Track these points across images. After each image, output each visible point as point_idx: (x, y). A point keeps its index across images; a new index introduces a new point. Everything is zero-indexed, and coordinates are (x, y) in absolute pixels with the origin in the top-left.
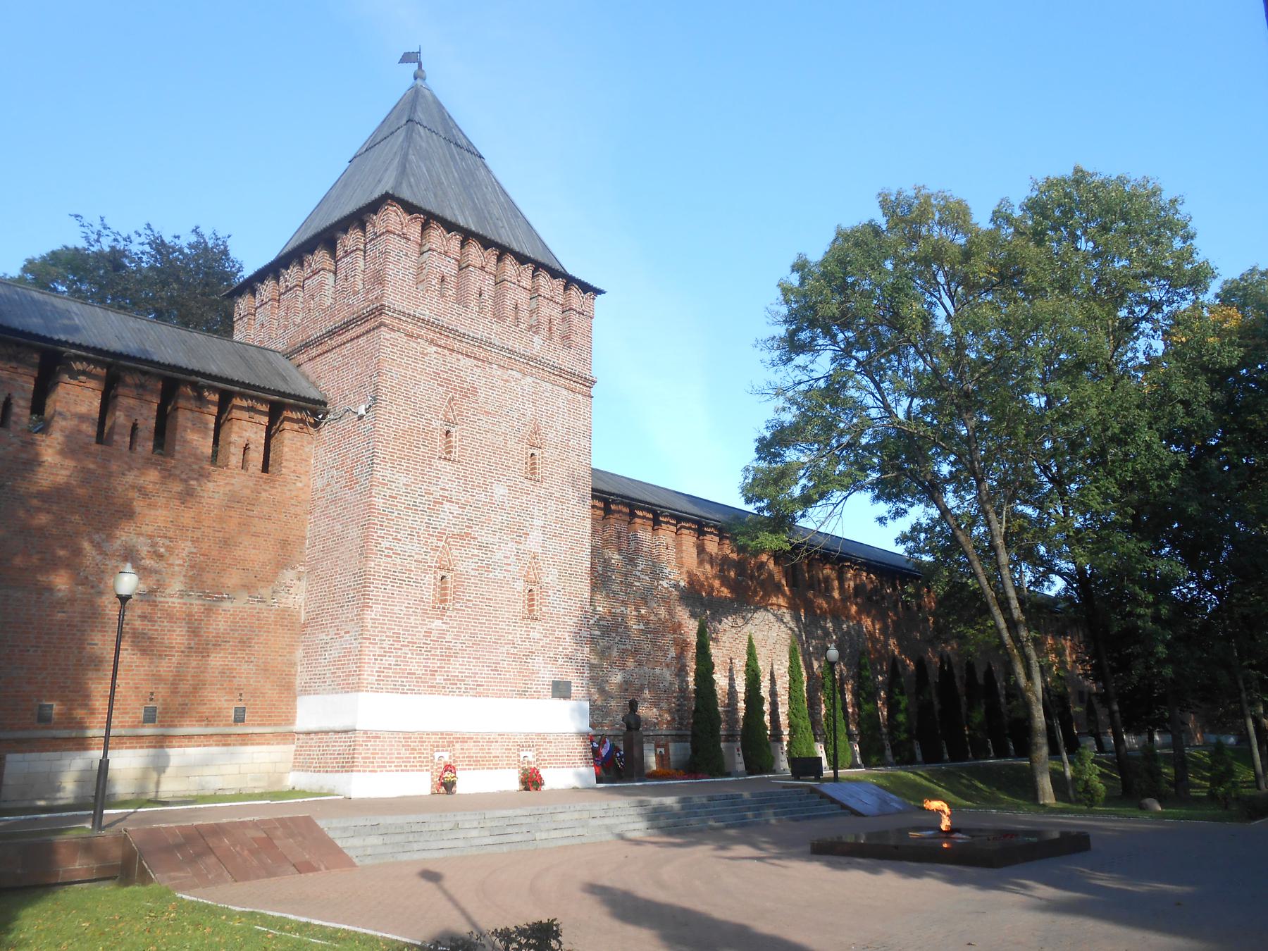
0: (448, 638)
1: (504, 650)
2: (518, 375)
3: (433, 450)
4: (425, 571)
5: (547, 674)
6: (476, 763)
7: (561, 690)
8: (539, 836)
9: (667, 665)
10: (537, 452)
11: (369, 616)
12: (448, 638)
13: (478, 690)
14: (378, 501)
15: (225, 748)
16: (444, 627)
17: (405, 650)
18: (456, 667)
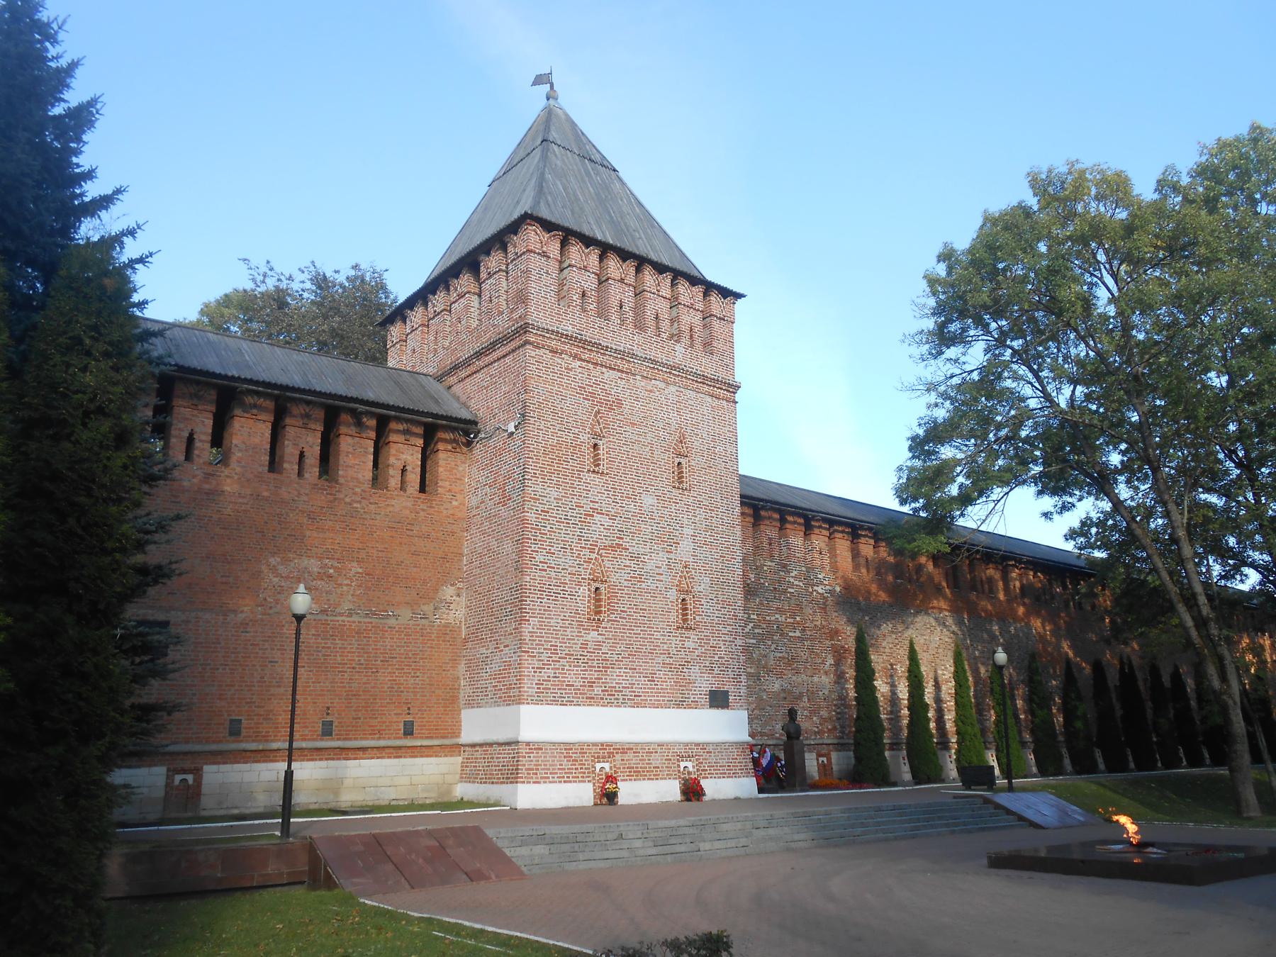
2: (662, 385)
3: (582, 463)
4: (579, 584)
5: (704, 684)
6: (637, 774)
7: (718, 700)
8: (705, 846)
9: (826, 673)
11: (526, 629)
14: (531, 516)
15: (397, 760)
18: (616, 677)
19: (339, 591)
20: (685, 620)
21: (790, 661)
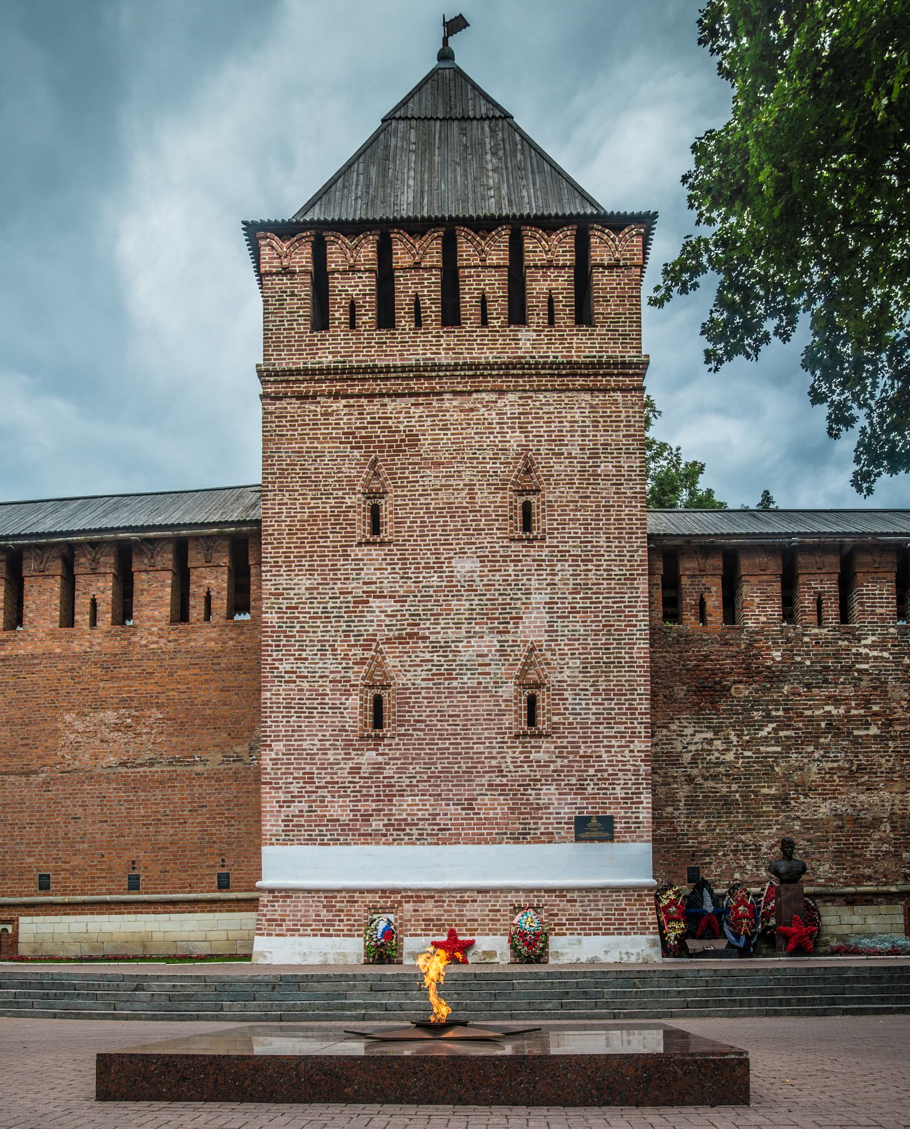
0: (387, 773)
1: (484, 781)
2: (494, 396)
3: (351, 535)
4: (347, 693)
7: (593, 828)
10: (533, 499)
11: (267, 759)
12: (387, 773)
13: (441, 835)
16: (380, 759)
17: (324, 792)
19: (138, 740)
20: (532, 721)
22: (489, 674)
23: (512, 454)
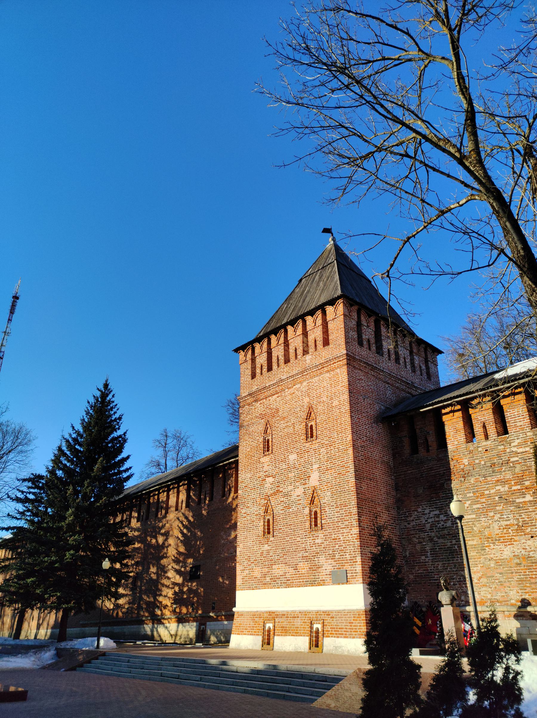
0: (271, 554)
1: (300, 555)
6: (285, 632)
13: (288, 583)
17: (253, 565)
21: (520, 528)
22: (301, 504)
23: (305, 407)
